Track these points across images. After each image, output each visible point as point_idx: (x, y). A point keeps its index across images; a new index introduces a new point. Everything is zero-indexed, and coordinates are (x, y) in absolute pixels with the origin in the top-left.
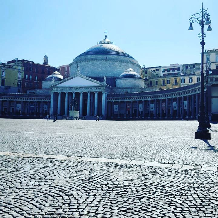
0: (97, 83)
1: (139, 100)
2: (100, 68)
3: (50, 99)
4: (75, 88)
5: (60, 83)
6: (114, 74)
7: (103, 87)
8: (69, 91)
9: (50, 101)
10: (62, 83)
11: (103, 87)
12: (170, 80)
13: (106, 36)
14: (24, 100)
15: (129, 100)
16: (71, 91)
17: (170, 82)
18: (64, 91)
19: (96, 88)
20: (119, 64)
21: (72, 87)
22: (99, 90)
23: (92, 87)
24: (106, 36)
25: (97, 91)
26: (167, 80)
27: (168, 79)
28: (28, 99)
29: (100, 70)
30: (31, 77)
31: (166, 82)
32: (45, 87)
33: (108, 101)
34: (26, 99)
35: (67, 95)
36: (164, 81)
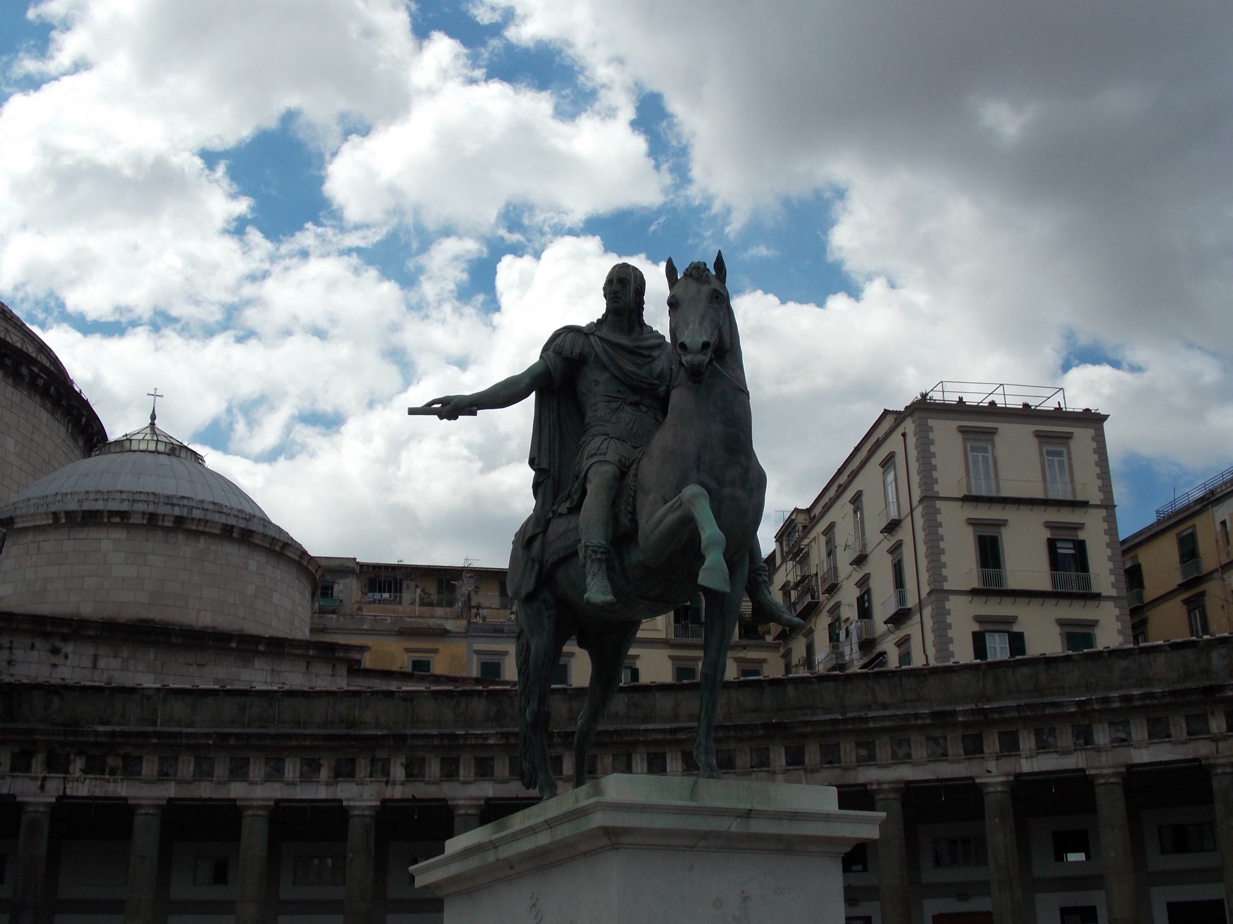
15: (322, 793)
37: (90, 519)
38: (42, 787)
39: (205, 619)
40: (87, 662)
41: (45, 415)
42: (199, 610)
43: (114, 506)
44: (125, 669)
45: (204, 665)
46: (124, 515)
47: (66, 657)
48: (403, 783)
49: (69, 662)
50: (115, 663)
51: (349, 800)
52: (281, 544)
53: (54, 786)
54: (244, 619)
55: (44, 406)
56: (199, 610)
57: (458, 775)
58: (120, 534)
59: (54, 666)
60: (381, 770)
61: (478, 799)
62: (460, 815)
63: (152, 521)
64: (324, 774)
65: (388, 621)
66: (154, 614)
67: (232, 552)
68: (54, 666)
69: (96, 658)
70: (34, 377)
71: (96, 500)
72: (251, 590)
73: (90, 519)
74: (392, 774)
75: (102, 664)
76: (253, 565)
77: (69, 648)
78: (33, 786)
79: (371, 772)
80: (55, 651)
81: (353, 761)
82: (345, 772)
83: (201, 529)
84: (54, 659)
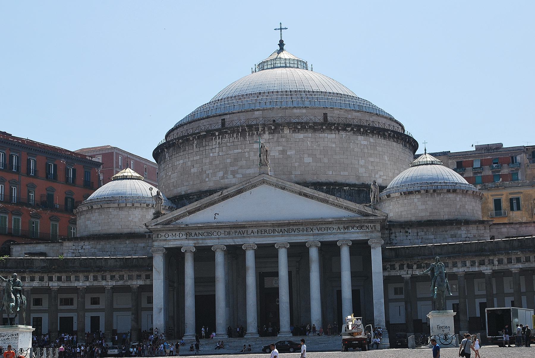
0: (347, 208)
1: (520, 266)
2: (309, 155)
3: (149, 277)
4: (255, 230)
5: (190, 213)
6: (358, 177)
7: (371, 222)
8: (231, 242)
9: (148, 282)
10: (198, 209)
11: (371, 222)
12: (521, 196)
13: (281, 44)
14: (36, 284)
15: (477, 269)
16: (238, 241)
17: (522, 202)
18: (209, 243)
19: (341, 226)
20: (372, 140)
21: (243, 227)
22: (357, 235)
23: (330, 223)
24: (281, 44)
25: (347, 236)
26: (511, 196)
27: (511, 194)
28: (51, 279)
29: (308, 160)
30: (15, 194)
31: (505, 205)
32: (100, 228)
33: (387, 274)
34: (42, 279)
35: (220, 258)
36: (498, 203)
37: (410, 193)
38: (407, 273)
39: (445, 217)
40: (415, 234)
41: (395, 144)
42: (444, 215)
43: (416, 188)
44: (425, 234)
45: (447, 231)
46: (419, 192)
47: (410, 233)
48: (497, 265)
49: (410, 235)
50: (423, 233)
51: (483, 270)
52: (466, 191)
53: (410, 272)
54: (457, 215)
55: (394, 141)
56: (444, 215)
57: (512, 263)
58: (419, 196)
59: (407, 236)
60: (491, 262)
61: (518, 268)
62: (514, 273)
63: (427, 191)
64: (477, 264)
65: (528, 182)
66: (431, 218)
67: (451, 196)
68: (407, 236)
69: (417, 233)
70: (390, 134)
71: (411, 187)
72: (458, 207)
73: (410, 193)
74: (494, 263)
75: (419, 234)
76: (458, 199)
77: (410, 231)
78: (405, 273)
79: (489, 263)
80: (407, 232)
81: (484, 260)
82: (482, 263)
83: (441, 192)
84: (407, 234)
